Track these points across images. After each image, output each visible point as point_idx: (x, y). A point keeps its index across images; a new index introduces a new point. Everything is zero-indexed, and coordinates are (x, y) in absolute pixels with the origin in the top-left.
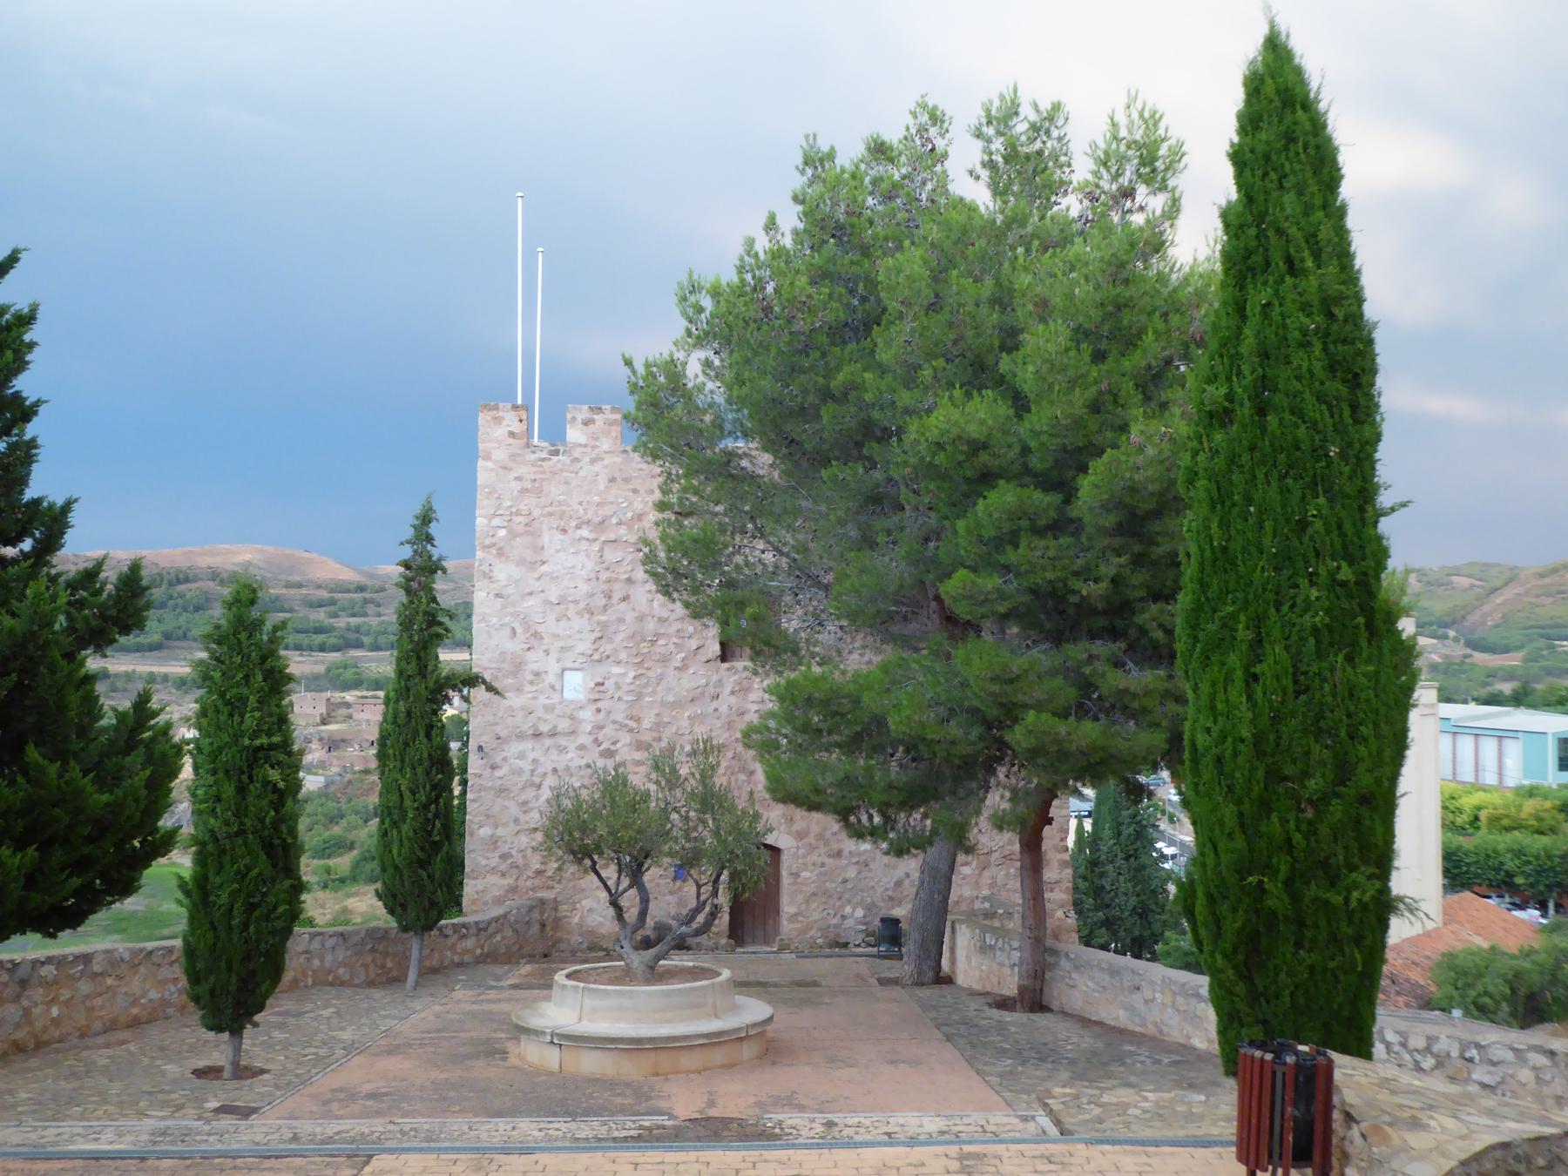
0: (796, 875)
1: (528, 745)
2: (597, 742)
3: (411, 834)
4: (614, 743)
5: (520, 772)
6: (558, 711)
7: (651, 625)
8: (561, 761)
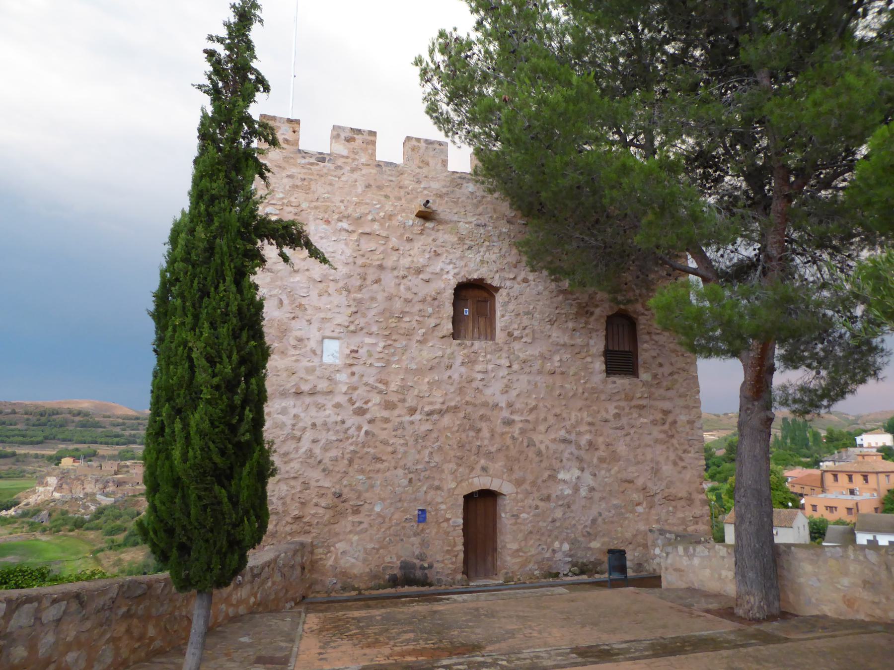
0: (516, 516)
1: (289, 402)
2: (351, 402)
3: (206, 425)
4: (366, 403)
5: (282, 426)
6: (318, 373)
7: (398, 305)
8: (320, 417)
